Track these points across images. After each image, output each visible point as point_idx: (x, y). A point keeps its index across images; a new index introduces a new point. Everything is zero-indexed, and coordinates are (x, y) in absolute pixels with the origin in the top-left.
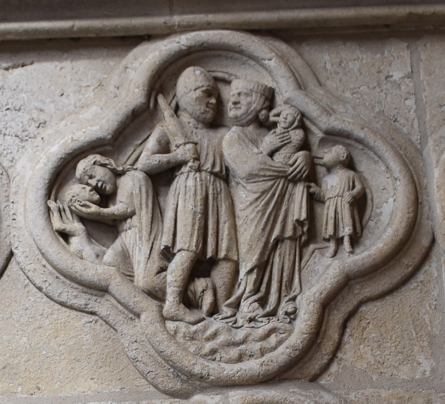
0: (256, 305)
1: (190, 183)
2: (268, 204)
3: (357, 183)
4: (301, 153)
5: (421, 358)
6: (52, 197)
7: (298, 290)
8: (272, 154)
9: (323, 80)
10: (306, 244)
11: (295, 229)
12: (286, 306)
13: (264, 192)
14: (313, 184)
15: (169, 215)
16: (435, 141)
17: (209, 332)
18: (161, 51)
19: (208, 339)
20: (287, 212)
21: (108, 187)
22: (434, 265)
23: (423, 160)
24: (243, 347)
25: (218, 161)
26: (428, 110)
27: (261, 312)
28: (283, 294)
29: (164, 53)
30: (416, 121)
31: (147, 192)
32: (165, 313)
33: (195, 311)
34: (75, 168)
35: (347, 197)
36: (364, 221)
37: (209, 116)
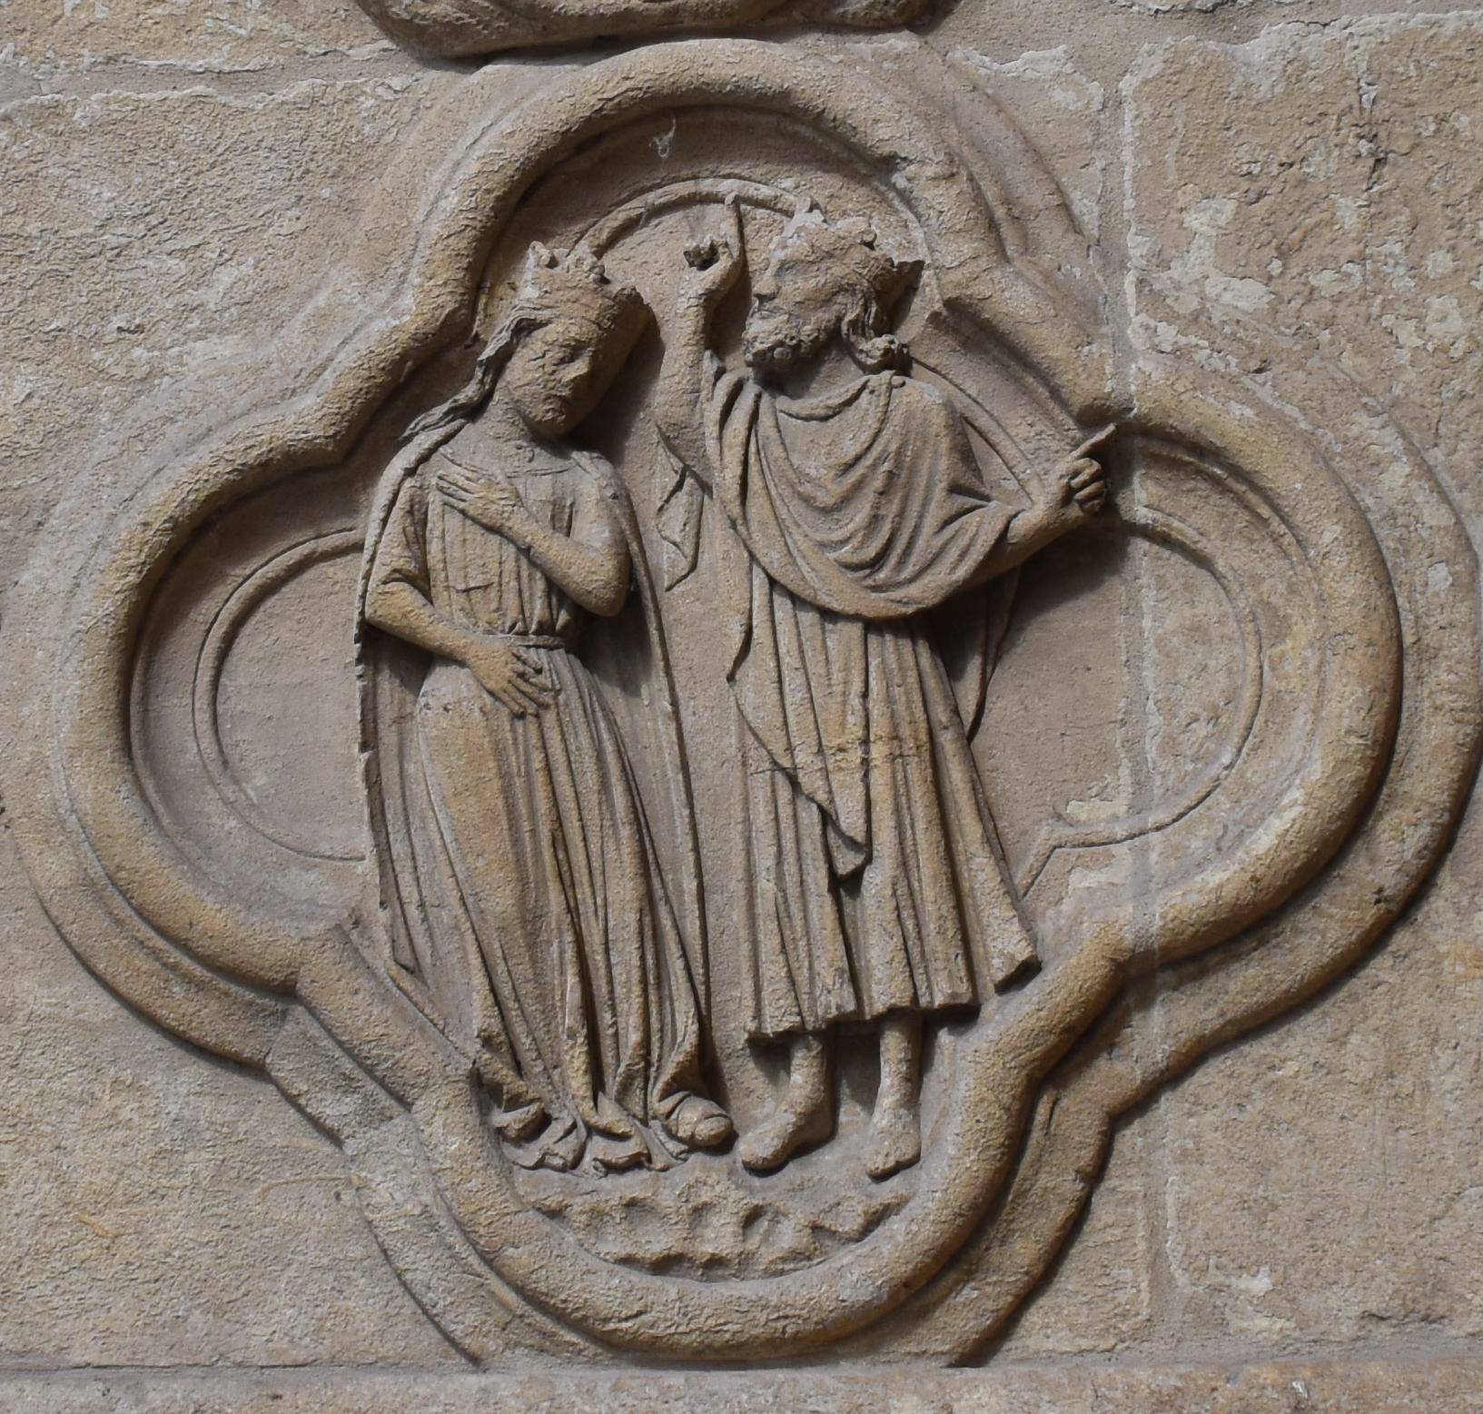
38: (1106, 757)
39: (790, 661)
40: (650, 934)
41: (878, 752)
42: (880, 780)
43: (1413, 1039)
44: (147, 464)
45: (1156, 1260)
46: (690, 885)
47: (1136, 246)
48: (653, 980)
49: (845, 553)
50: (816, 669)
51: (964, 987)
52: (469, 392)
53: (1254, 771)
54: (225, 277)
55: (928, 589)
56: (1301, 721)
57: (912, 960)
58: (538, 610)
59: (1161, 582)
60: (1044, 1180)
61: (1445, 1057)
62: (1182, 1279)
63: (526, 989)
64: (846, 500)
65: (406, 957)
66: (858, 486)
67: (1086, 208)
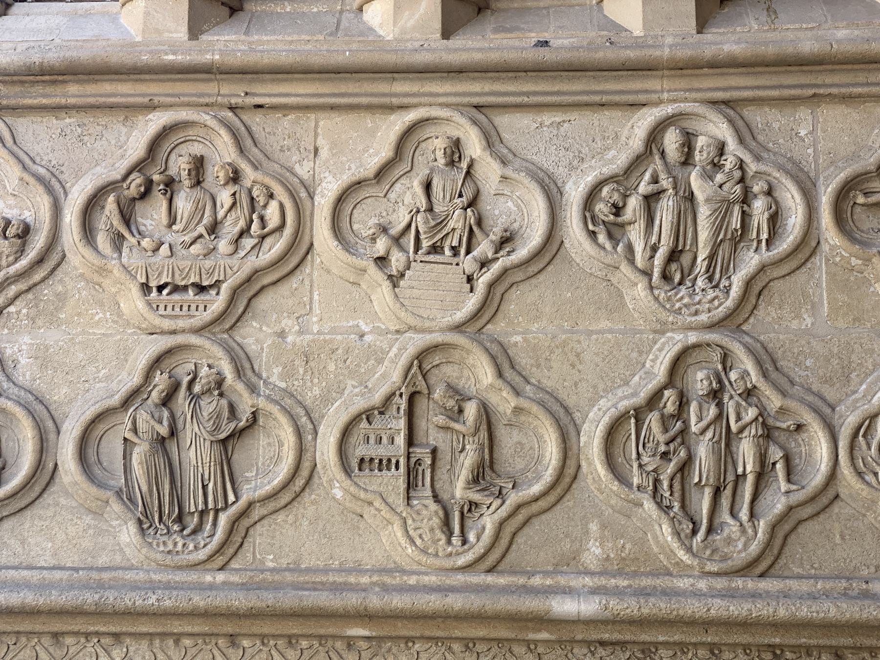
0: (707, 281)
1: (671, 203)
2: (717, 218)
3: (773, 205)
4: (739, 185)
5: (805, 316)
6: (587, 209)
7: (732, 271)
8: (720, 186)
9: (755, 135)
10: (740, 241)
11: (733, 233)
12: (724, 283)
13: (715, 211)
14: (745, 206)
15: (657, 222)
16: (824, 178)
17: (678, 296)
18: (655, 116)
19: (678, 301)
20: (728, 222)
21: (621, 205)
22: (818, 258)
23: (816, 191)
24: (698, 306)
25: (687, 188)
26: (821, 156)
27: (710, 285)
28: (723, 274)
29: (657, 118)
30: (813, 164)
31: (644, 209)
32: (653, 285)
33: (670, 282)
34: (601, 190)
35: (766, 215)
36: (776, 229)
37: (683, 159)
38: (252, 465)
39: (198, 447)
40: (171, 494)
41: (212, 464)
42: (212, 469)
43: (300, 516)
44: (87, 407)
45: (254, 553)
46: (180, 485)
47: (264, 375)
48: (171, 503)
49: (208, 429)
50: (203, 449)
51: (224, 505)
52: (146, 396)
53: (276, 469)
54: (103, 371)
55: (223, 436)
56: (285, 460)
57: (215, 501)
58: (155, 436)
59: (264, 436)
60: (235, 539)
61: (305, 520)
62: (258, 556)
63: (149, 503)
64: (209, 419)
65: (129, 497)
66: (212, 417)
67: (256, 367)
